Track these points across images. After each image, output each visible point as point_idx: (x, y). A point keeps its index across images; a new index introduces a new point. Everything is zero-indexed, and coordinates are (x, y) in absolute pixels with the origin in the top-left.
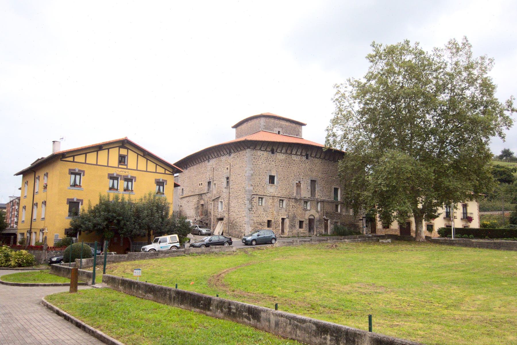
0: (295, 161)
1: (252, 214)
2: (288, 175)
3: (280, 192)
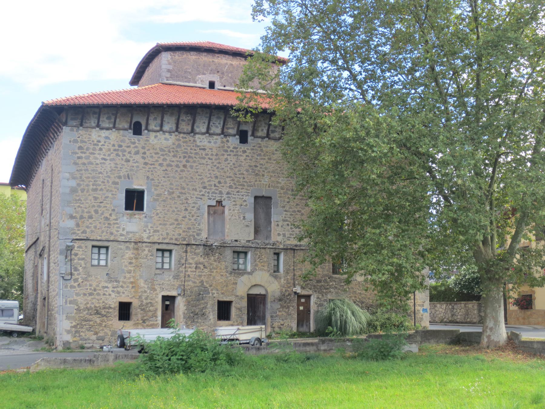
0: (204, 149)
1: (72, 287)
2: (184, 185)
3: (158, 231)
